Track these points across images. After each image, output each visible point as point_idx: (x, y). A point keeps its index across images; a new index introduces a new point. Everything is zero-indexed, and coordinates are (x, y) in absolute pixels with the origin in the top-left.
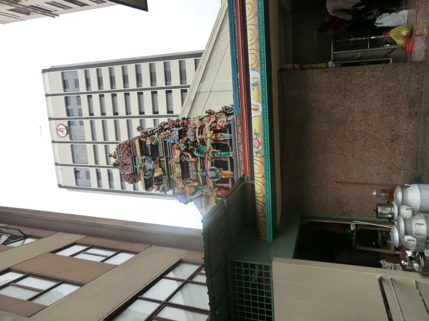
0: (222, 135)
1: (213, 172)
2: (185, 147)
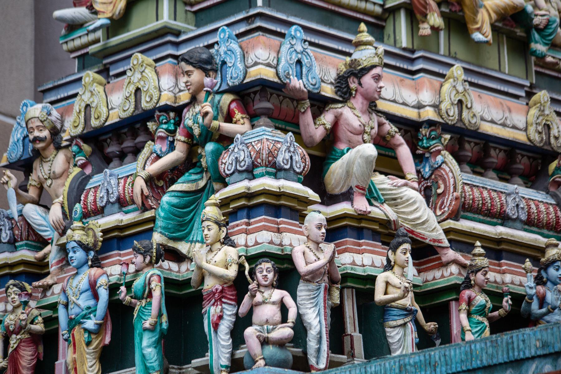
0: (216, 326)
1: (84, 301)
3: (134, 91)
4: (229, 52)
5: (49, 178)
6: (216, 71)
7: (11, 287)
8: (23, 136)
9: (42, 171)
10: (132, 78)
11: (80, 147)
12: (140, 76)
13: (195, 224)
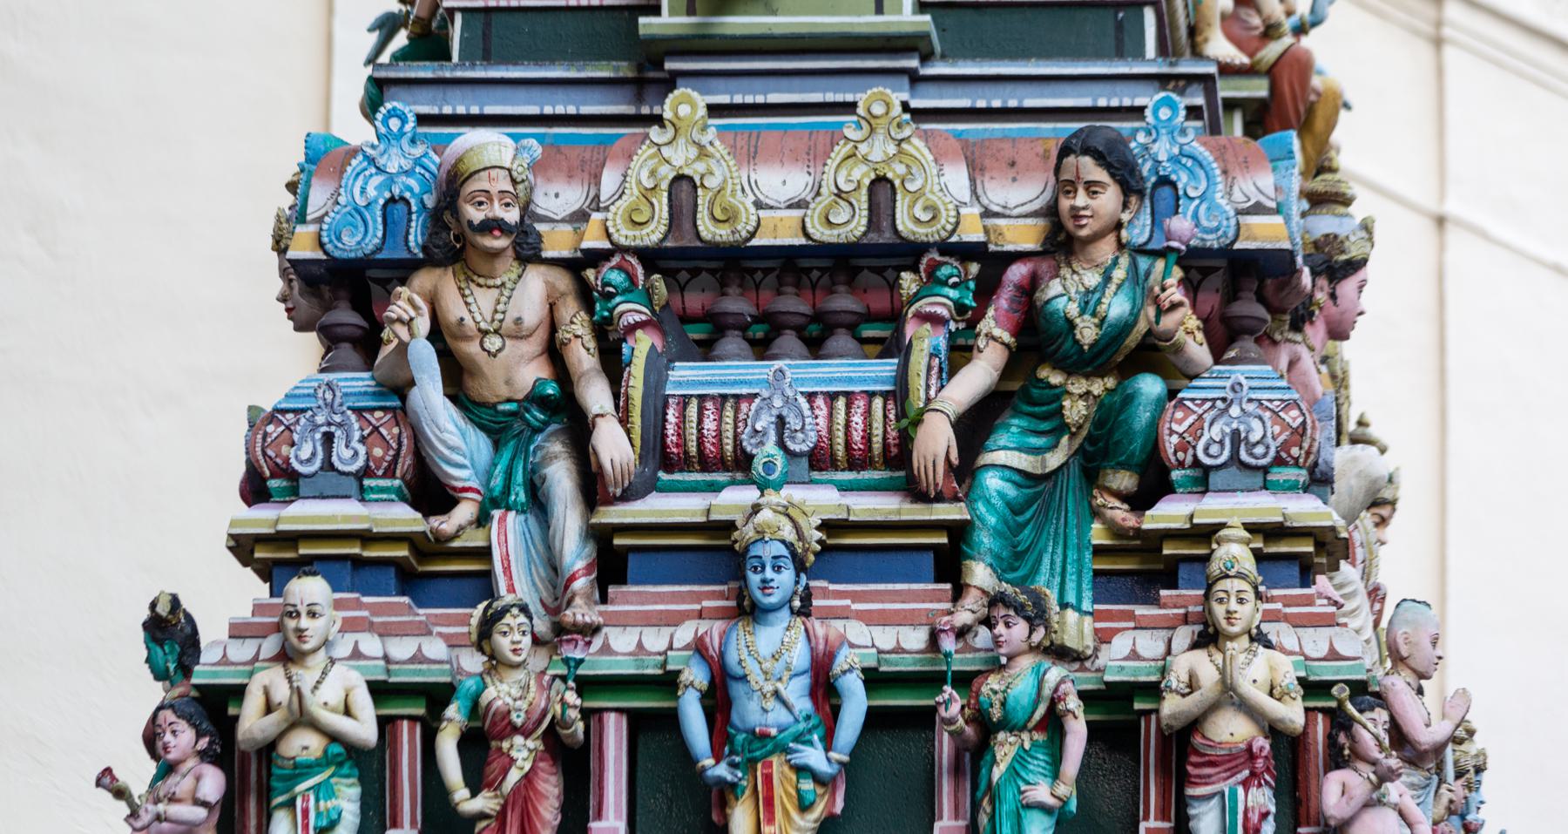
2: (1088, 333)
3: (867, 182)
4: (1189, 163)
5: (496, 332)
6: (1141, 194)
7: (515, 611)
8: (387, 195)
9: (474, 308)
10: (863, 148)
11: (632, 278)
12: (892, 149)
13: (1046, 560)
